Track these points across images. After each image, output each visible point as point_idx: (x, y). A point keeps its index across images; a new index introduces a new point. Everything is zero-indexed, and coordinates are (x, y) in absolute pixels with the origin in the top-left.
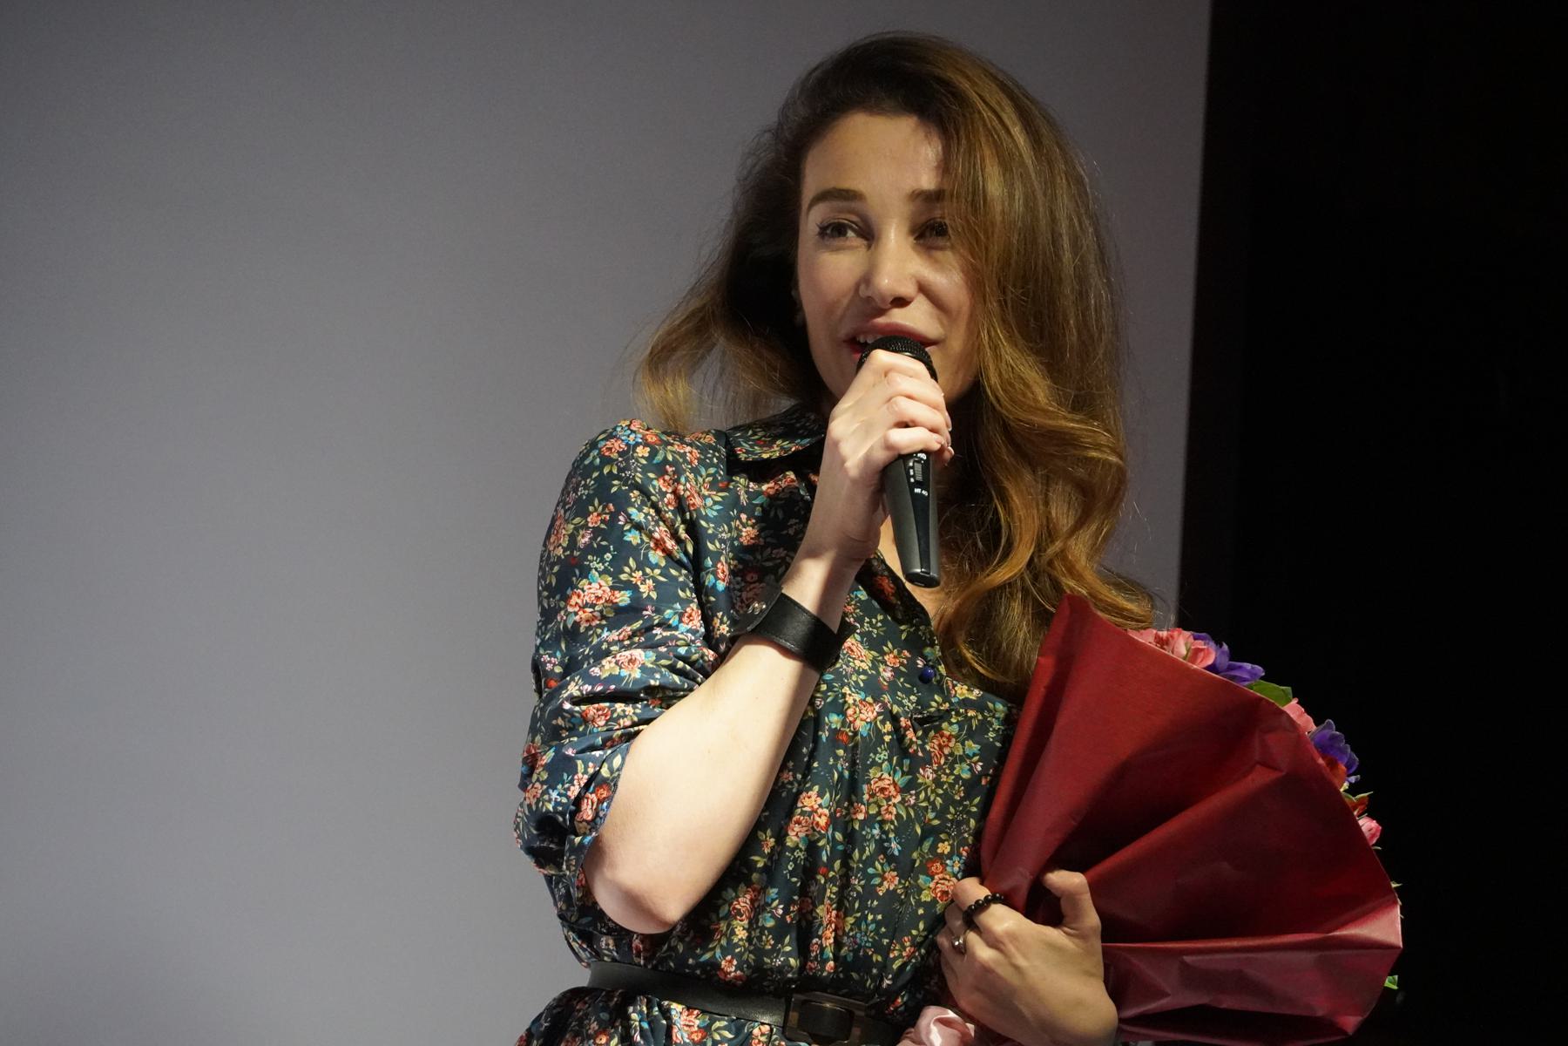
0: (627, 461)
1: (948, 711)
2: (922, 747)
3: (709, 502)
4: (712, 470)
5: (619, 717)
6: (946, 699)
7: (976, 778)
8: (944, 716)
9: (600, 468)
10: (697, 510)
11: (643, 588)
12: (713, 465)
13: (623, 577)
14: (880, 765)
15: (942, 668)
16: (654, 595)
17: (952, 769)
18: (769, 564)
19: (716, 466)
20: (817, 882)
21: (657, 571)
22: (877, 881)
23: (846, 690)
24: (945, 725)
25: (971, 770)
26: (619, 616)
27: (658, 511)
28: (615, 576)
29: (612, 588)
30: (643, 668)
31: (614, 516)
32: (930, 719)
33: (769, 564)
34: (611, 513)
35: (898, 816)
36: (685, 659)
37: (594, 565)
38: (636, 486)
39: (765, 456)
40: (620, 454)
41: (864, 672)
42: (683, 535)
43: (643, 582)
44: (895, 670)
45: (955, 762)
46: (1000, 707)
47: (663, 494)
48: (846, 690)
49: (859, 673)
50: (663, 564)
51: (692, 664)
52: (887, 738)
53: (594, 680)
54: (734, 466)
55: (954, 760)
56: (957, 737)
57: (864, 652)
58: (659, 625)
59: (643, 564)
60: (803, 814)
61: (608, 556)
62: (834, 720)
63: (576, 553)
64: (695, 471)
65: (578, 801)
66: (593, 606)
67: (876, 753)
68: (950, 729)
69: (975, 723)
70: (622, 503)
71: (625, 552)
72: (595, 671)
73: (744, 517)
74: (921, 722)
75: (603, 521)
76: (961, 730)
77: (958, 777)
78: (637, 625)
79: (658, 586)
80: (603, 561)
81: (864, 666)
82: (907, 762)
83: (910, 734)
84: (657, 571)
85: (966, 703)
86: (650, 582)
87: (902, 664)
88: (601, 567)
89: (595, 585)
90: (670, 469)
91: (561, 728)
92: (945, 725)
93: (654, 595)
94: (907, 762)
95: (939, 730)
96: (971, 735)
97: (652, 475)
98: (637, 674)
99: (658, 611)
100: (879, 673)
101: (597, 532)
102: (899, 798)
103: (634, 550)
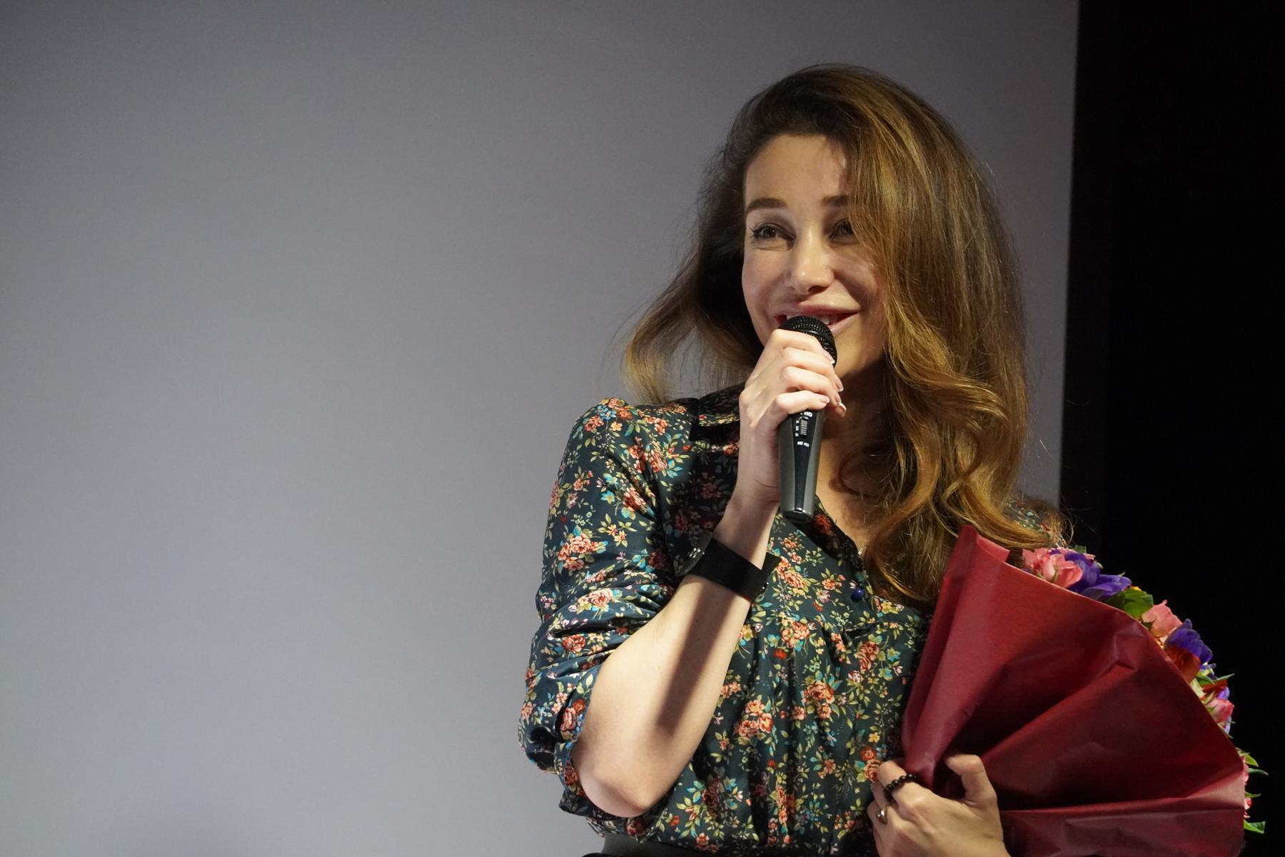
0: (603, 434)
1: (874, 625)
2: (851, 656)
3: (672, 464)
4: (677, 436)
5: (592, 644)
6: (873, 615)
7: (897, 679)
8: (870, 629)
9: (583, 442)
10: (660, 473)
11: (617, 539)
12: (679, 432)
14: (813, 674)
15: (869, 589)
16: (625, 544)
17: (877, 672)
19: (683, 432)
20: (767, 772)
21: (629, 524)
23: (782, 615)
24: (871, 636)
25: (893, 673)
26: (597, 561)
27: (628, 475)
28: (594, 529)
29: (593, 540)
30: (611, 603)
31: (593, 481)
32: (859, 632)
34: (590, 479)
36: (647, 595)
39: (721, 422)
40: (599, 429)
41: (801, 598)
42: (650, 493)
43: (617, 533)
44: (831, 592)
45: (879, 667)
46: (917, 618)
47: (633, 461)
48: (782, 615)
49: (795, 599)
50: (634, 517)
51: (653, 598)
52: (820, 651)
53: (571, 616)
55: (879, 665)
56: (880, 646)
57: (802, 580)
58: (629, 568)
59: (617, 519)
60: (751, 718)
61: (589, 514)
62: (773, 639)
63: (565, 513)
64: (662, 439)
65: (560, 717)
66: (577, 555)
67: (809, 664)
68: (874, 639)
69: (896, 634)
70: (599, 470)
71: (602, 509)
72: (573, 608)
73: (705, 475)
74: (852, 635)
75: (585, 486)
76: (884, 640)
77: (882, 679)
78: (610, 568)
79: (629, 536)
80: (585, 518)
81: (801, 593)
82: (838, 669)
83: (840, 647)
84: (629, 524)
85: (890, 617)
86: (622, 533)
87: (837, 587)
88: (583, 523)
89: (578, 538)
90: (639, 440)
91: (547, 655)
92: (871, 636)
93: (625, 544)
95: (866, 640)
96: (893, 643)
97: (623, 446)
98: (606, 609)
99: (629, 557)
100: (815, 597)
101: (580, 494)
103: (608, 508)
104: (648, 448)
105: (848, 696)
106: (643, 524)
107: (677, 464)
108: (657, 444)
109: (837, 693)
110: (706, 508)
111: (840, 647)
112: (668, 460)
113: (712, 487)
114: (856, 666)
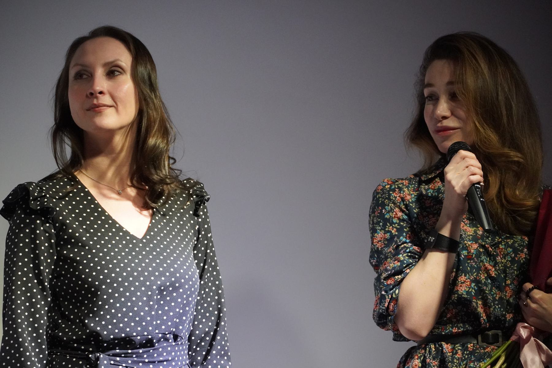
1: (501, 241)
4: (413, 186)
8: (500, 243)
10: (409, 201)
11: (393, 231)
12: (413, 184)
13: (387, 229)
16: (397, 233)
18: (435, 212)
19: (415, 184)
21: (396, 225)
22: (495, 295)
25: (511, 257)
28: (384, 230)
29: (384, 234)
31: (381, 211)
33: (435, 212)
35: (495, 274)
37: (377, 228)
38: (386, 198)
41: (471, 235)
43: (393, 230)
54: (420, 183)
57: (470, 229)
59: (392, 223)
61: (381, 224)
66: (381, 241)
74: (493, 245)
75: (378, 213)
79: (398, 230)
80: (380, 226)
81: (471, 233)
82: (492, 258)
83: (490, 249)
84: (396, 225)
86: (395, 229)
88: (380, 228)
92: (500, 245)
94: (492, 258)
95: (498, 247)
100: (477, 234)
102: (494, 269)
104: (402, 192)
105: (499, 266)
106: (402, 223)
107: (415, 196)
108: (406, 190)
109: (494, 266)
110: (428, 210)
111: (490, 249)
112: (411, 195)
113: (429, 202)
114: (497, 255)
